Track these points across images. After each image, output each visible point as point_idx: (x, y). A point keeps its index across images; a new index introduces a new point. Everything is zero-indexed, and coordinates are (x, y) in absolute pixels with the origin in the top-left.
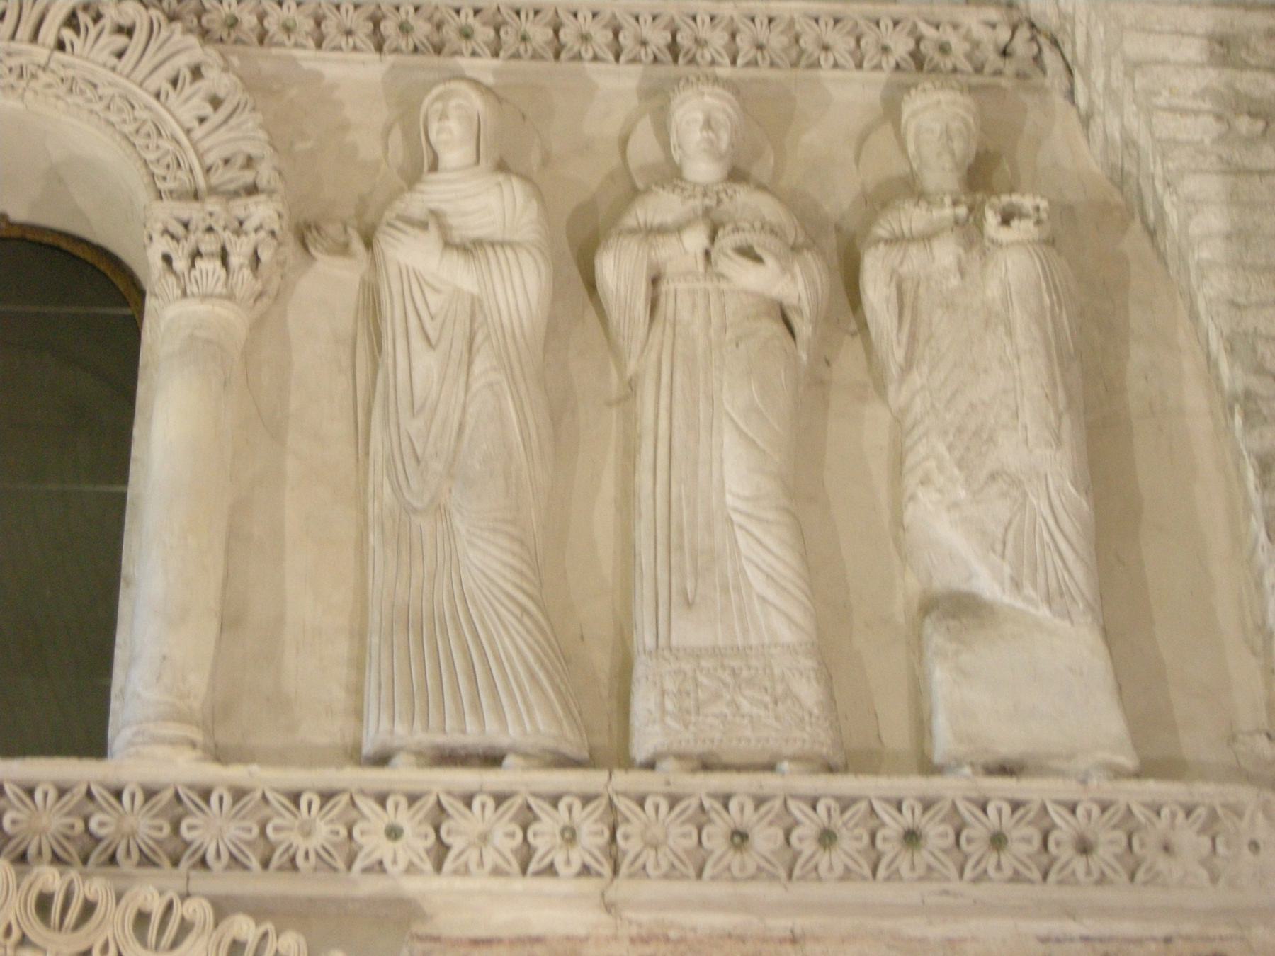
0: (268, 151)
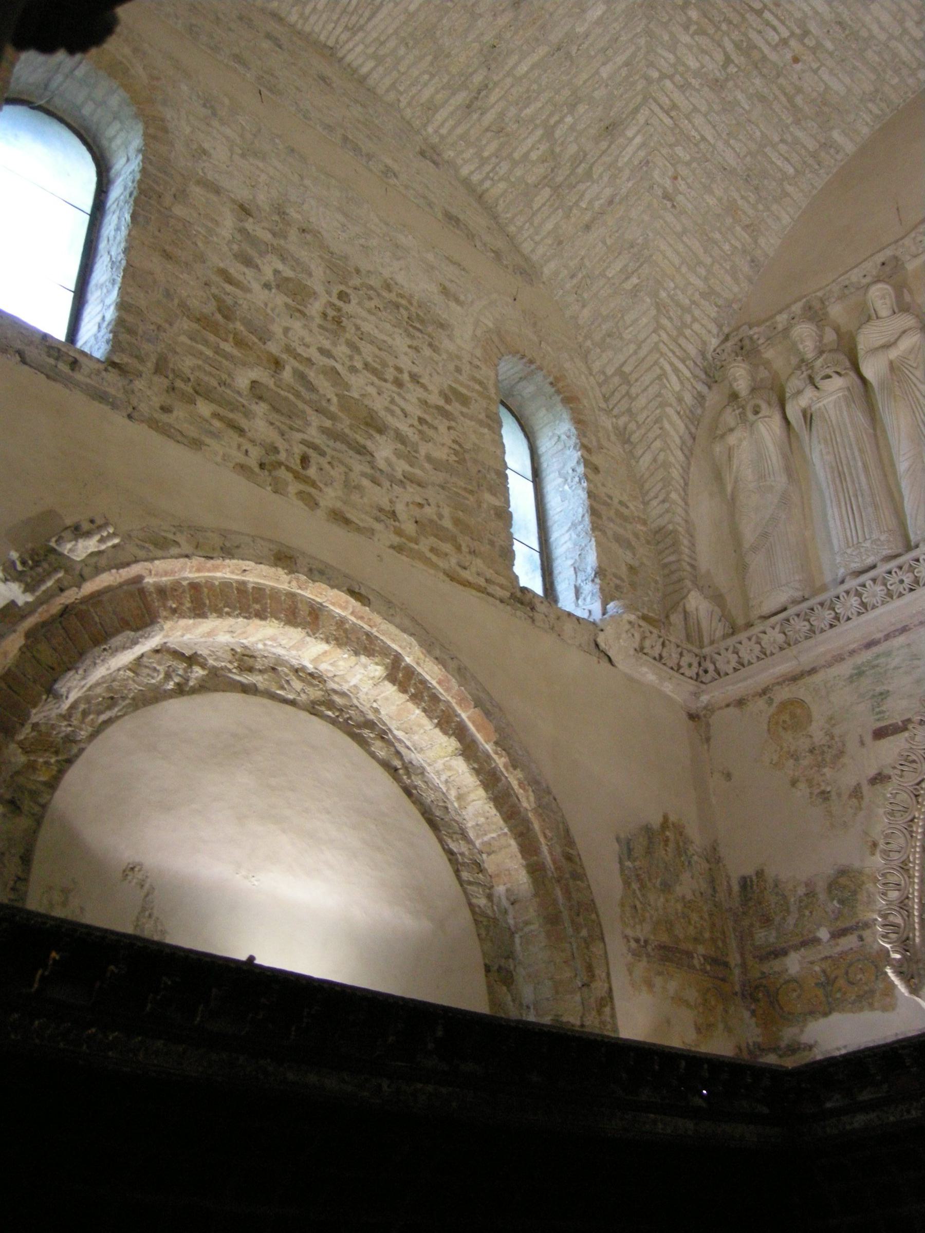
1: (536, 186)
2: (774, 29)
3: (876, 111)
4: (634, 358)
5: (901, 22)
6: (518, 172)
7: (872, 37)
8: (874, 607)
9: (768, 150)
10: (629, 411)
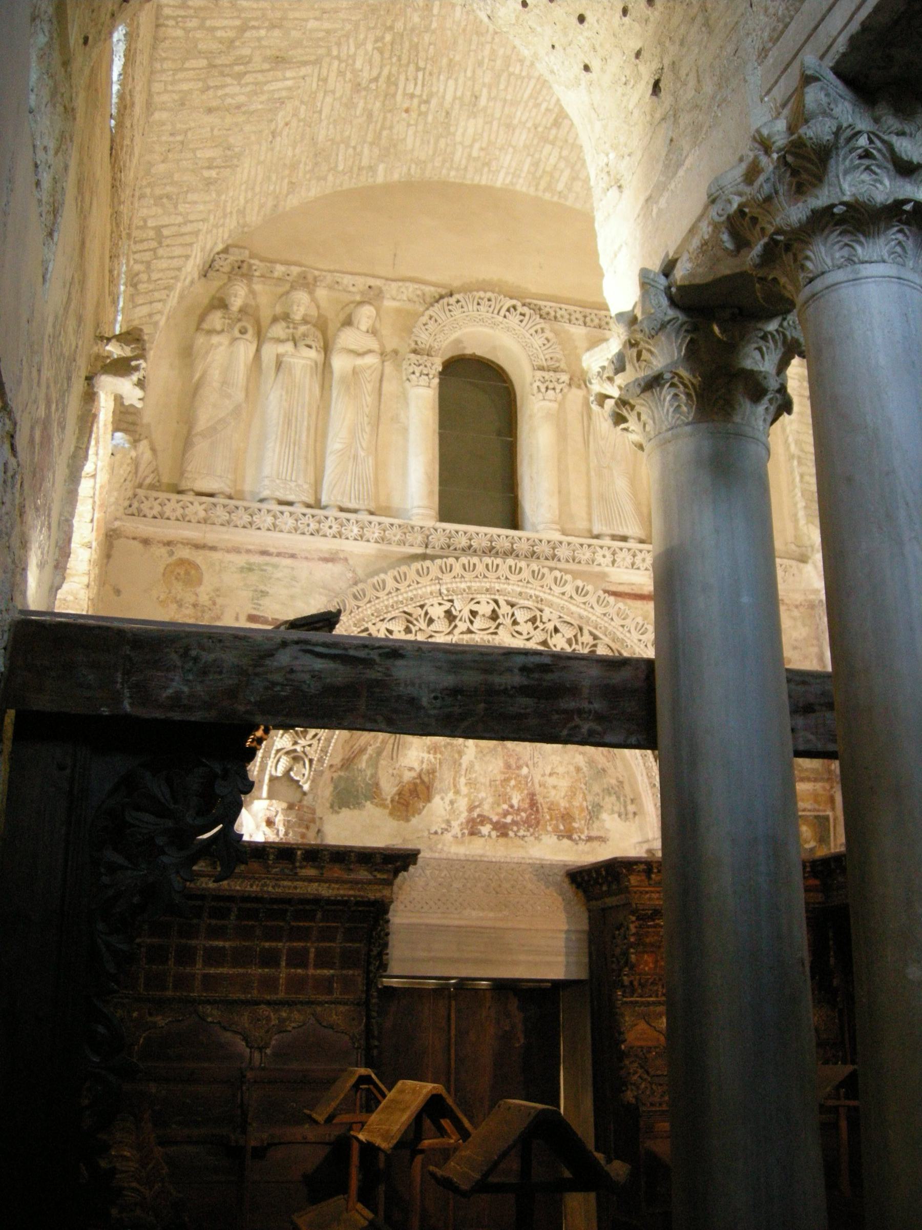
0: (563, 358)
1: (199, 52)
2: (416, 84)
3: (412, 171)
4: (176, 228)
5: (474, 141)
6: (199, 34)
7: (454, 135)
8: (281, 531)
9: (342, 146)
10: (148, 264)
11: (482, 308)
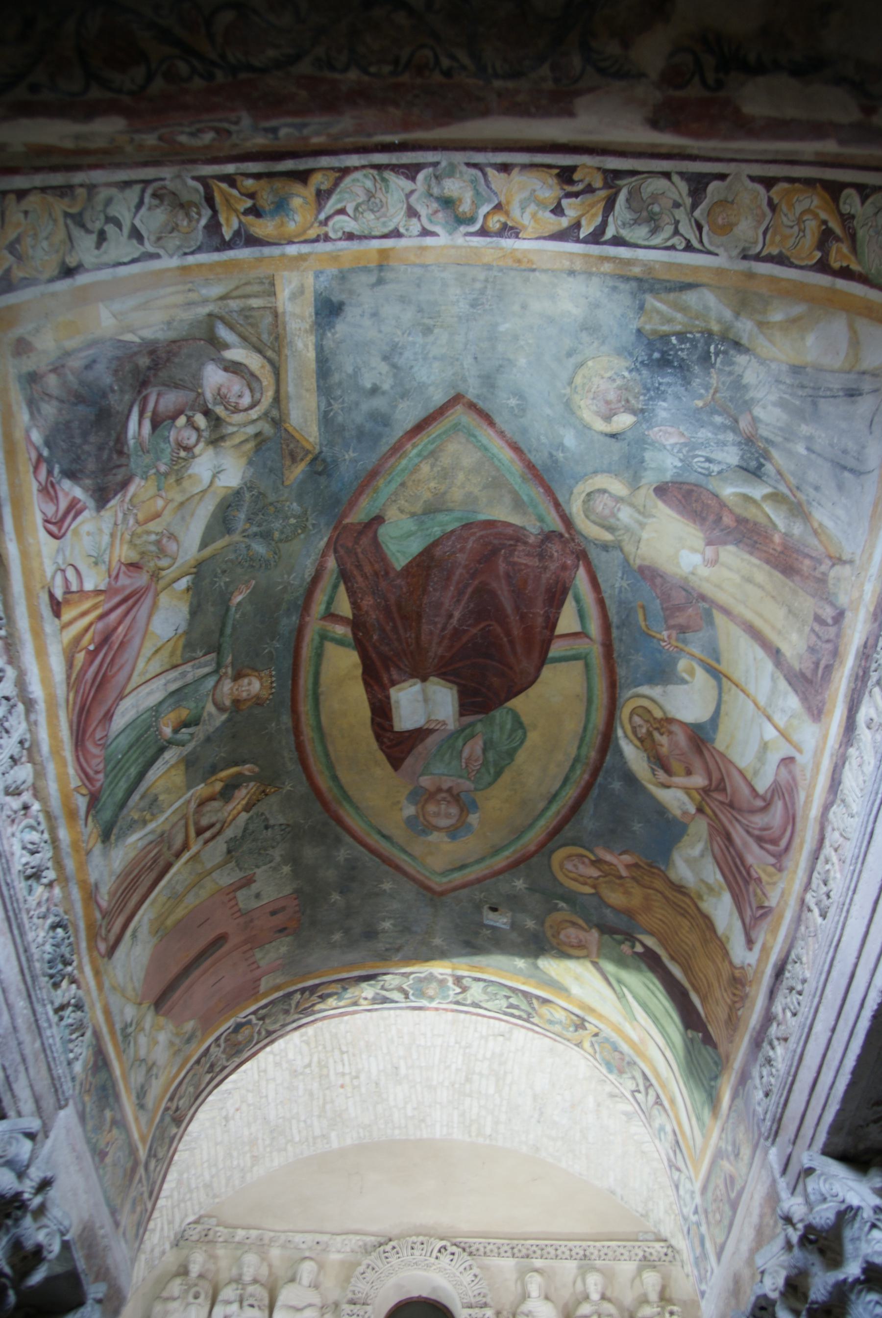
11: (415, 1251)
